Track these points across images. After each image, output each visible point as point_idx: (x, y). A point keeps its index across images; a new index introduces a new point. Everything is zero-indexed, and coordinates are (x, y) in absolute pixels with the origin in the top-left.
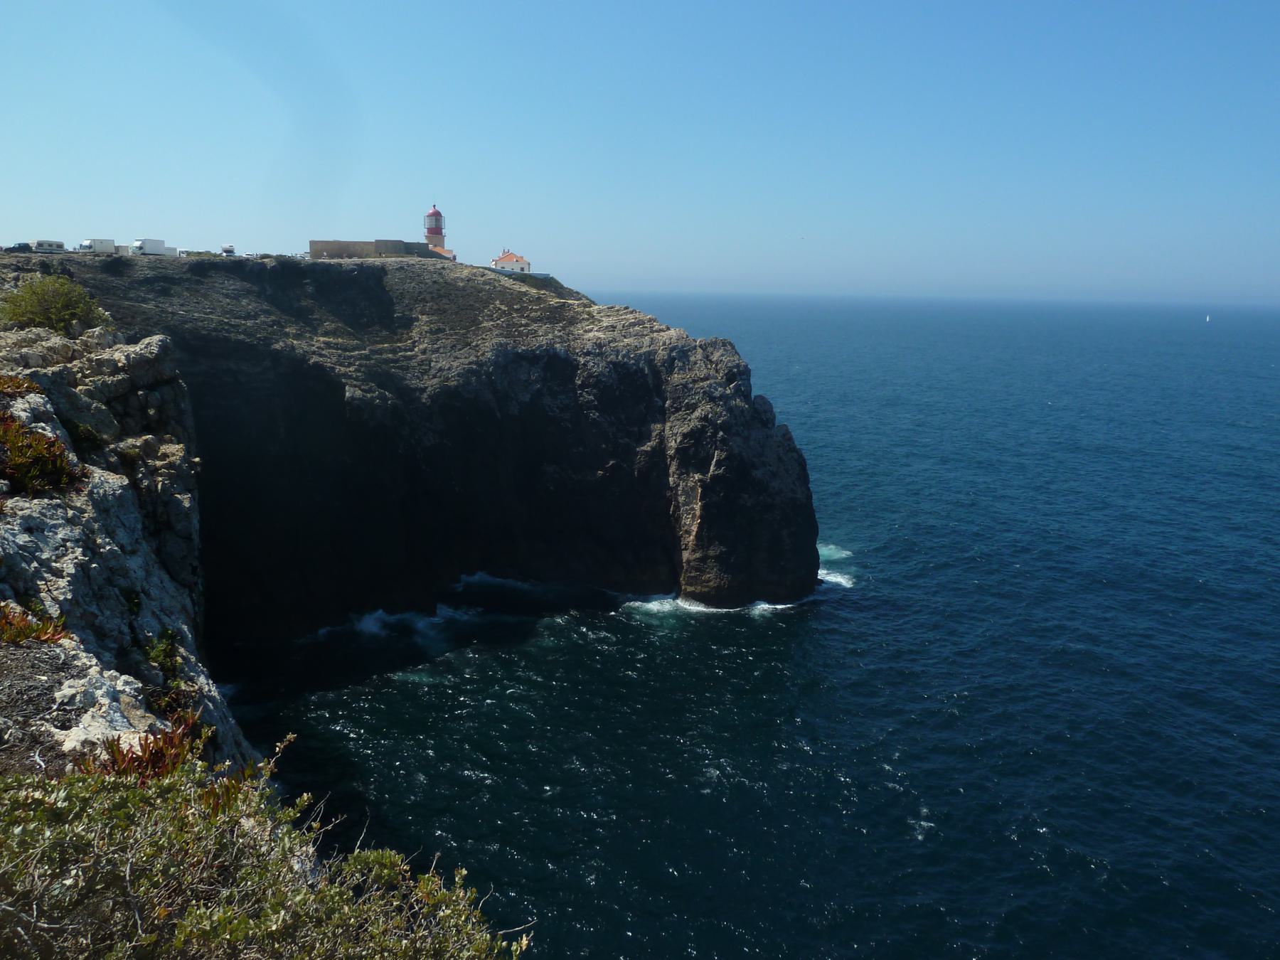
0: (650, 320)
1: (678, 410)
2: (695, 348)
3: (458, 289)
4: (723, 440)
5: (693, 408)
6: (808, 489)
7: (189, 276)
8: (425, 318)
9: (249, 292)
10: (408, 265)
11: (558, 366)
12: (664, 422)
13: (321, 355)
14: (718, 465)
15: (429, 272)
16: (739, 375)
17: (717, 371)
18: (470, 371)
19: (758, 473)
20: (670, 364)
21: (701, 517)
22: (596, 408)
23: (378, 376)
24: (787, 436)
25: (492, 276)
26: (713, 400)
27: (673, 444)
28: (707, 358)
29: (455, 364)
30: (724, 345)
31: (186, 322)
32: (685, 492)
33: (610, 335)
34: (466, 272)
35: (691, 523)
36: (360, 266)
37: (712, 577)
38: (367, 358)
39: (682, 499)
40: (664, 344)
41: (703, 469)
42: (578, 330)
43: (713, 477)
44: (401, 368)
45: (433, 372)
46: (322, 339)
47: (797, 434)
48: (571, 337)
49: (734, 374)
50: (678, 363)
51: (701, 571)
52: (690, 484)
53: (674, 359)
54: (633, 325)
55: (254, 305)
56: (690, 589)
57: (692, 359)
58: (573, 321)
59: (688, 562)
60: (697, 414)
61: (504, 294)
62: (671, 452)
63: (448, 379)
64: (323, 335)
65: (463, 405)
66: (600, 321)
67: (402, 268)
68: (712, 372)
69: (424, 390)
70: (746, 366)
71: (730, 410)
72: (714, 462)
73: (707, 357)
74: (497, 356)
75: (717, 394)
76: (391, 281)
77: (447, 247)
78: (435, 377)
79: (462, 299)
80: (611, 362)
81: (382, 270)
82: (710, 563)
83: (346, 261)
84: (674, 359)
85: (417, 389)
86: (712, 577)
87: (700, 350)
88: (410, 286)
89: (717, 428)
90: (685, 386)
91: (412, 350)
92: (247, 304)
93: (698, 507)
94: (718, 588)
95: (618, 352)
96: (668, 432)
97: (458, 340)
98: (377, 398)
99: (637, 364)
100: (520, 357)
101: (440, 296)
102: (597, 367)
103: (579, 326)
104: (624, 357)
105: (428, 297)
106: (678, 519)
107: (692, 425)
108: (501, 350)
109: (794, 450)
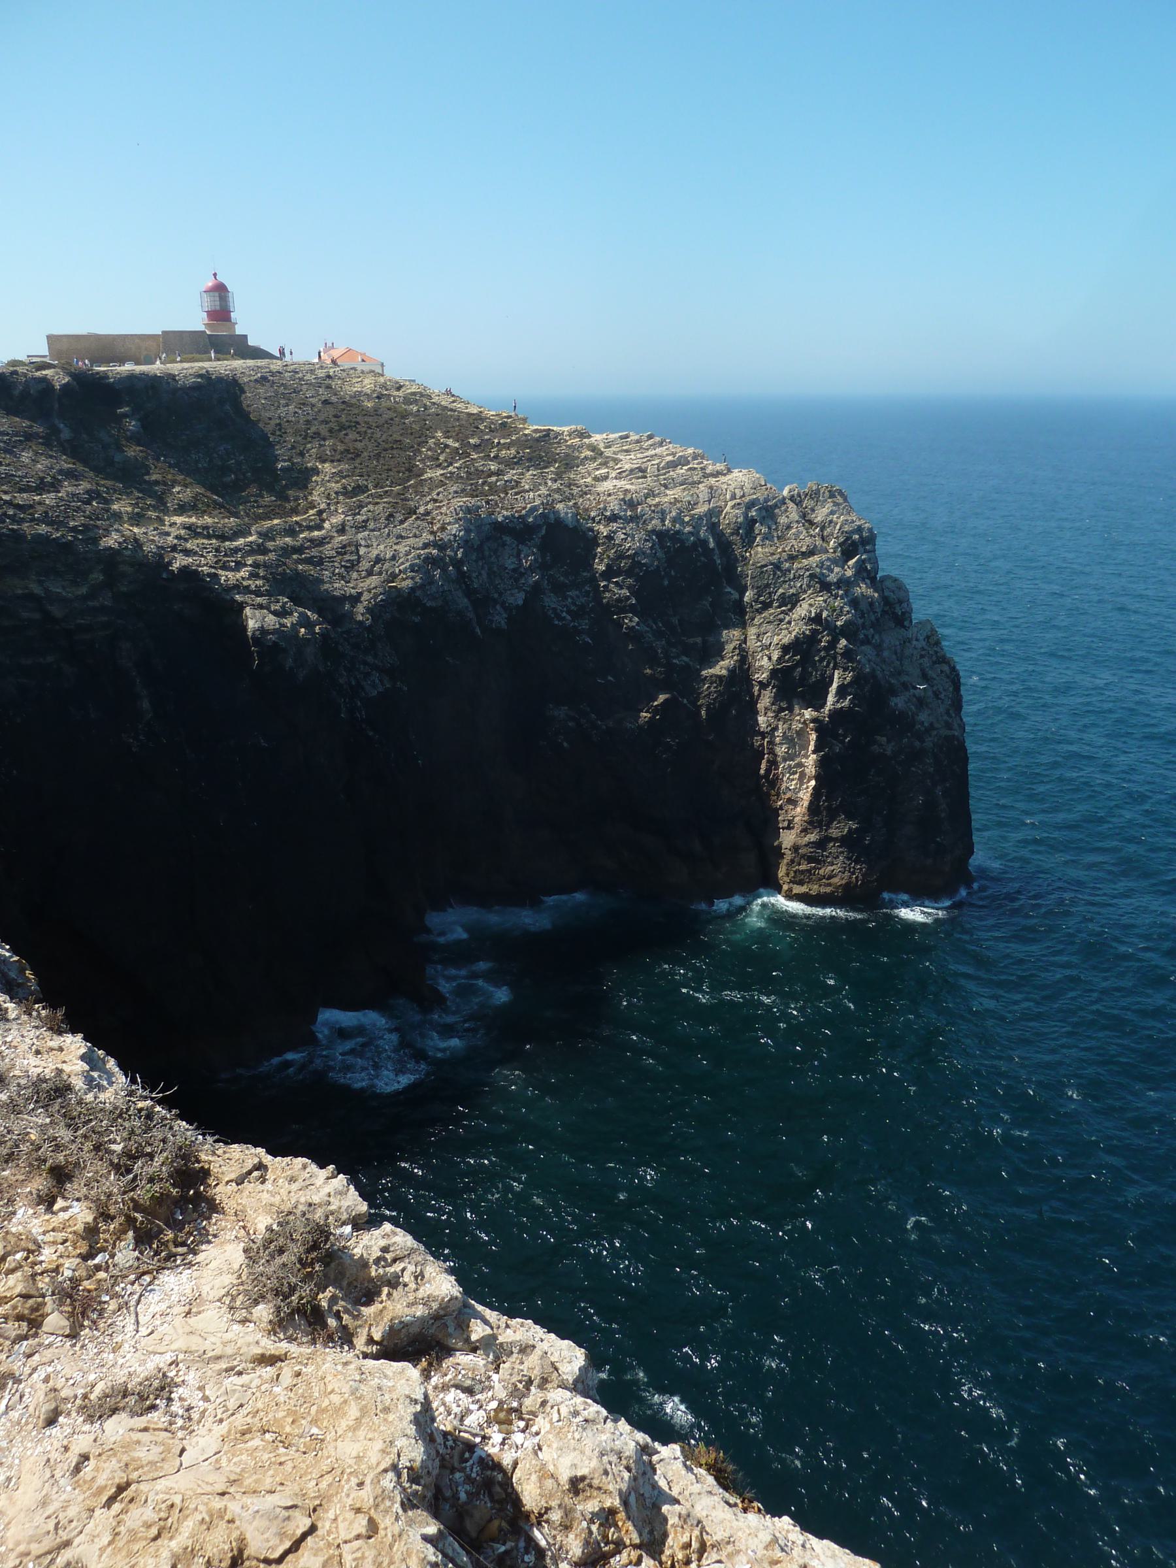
0: (695, 457)
1: (766, 606)
3: (366, 413)
4: (848, 654)
5: (792, 601)
9: (29, 437)
10: (273, 374)
11: (563, 542)
12: (743, 625)
13: (187, 552)
14: (842, 692)
17: (823, 539)
18: (428, 559)
19: (898, 702)
21: (817, 778)
22: (633, 609)
23: (290, 584)
24: (933, 640)
26: (825, 586)
27: (765, 662)
29: (402, 549)
30: (832, 496)
34: (368, 384)
37: (837, 870)
38: (261, 550)
39: (781, 750)
40: (733, 497)
41: (815, 698)
42: (584, 475)
43: (834, 714)
44: (309, 561)
45: (365, 565)
46: (179, 520)
49: (854, 543)
52: (797, 726)
53: (754, 521)
54: (673, 465)
55: (47, 462)
56: (798, 890)
57: (783, 520)
58: (569, 463)
59: (795, 848)
60: (802, 610)
62: (763, 676)
63: (393, 577)
66: (617, 461)
67: (264, 378)
68: (819, 542)
69: (356, 599)
71: (854, 603)
72: (835, 685)
73: (804, 516)
74: (468, 531)
75: (832, 578)
76: (255, 401)
78: (370, 573)
79: (385, 433)
80: (653, 531)
81: (231, 388)
83: (175, 368)
84: (754, 521)
85: (344, 598)
86: (837, 870)
87: (791, 505)
88: (287, 411)
90: (777, 566)
91: (319, 527)
92: (34, 462)
93: (810, 761)
94: (847, 887)
95: (663, 512)
96: (752, 643)
99: (695, 533)
100: (500, 529)
101: (342, 427)
102: (632, 540)
104: (674, 521)
106: (774, 782)
109: (943, 660)
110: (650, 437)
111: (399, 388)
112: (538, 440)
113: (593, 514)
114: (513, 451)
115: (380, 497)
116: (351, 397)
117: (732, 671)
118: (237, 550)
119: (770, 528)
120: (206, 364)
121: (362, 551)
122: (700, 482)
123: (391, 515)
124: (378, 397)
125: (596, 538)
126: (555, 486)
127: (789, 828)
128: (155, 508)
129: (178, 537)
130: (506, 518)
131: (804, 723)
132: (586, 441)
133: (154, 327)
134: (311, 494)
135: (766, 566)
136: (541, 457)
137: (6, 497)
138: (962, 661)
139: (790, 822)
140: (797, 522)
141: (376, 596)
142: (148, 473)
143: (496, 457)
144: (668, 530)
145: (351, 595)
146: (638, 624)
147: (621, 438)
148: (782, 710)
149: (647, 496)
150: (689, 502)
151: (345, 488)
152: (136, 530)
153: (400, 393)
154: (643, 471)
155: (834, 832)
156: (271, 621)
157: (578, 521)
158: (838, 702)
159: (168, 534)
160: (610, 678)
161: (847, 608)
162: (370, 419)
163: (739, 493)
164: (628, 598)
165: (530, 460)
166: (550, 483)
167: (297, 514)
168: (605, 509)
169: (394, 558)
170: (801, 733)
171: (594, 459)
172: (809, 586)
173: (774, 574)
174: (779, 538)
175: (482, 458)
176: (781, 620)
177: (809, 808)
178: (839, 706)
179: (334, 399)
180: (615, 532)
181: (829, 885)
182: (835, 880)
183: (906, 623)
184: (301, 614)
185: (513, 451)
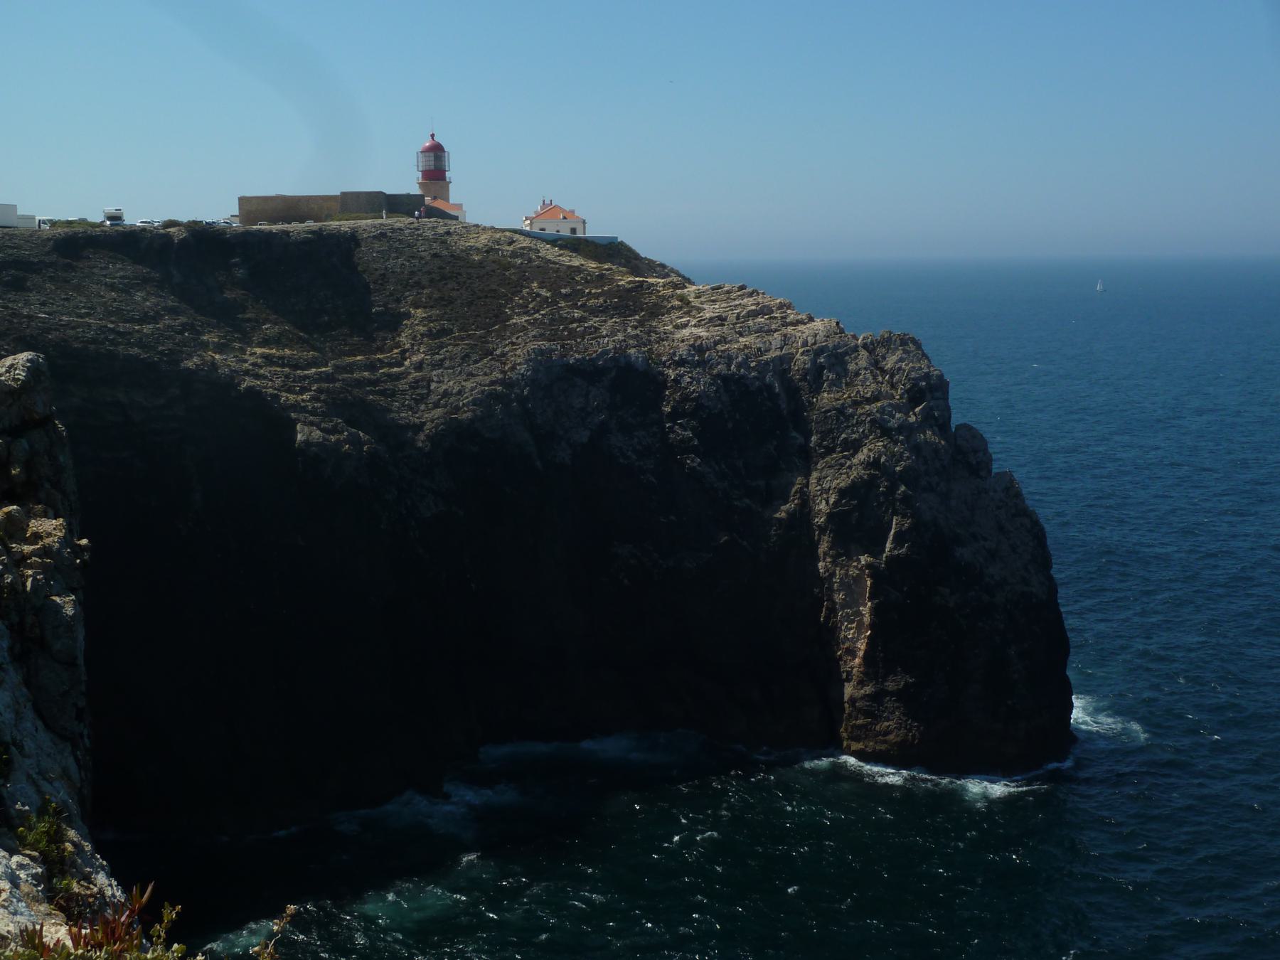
0: (781, 306)
1: (830, 451)
2: (856, 349)
4: (905, 499)
5: (854, 446)
6: (1051, 578)
7: (54, 257)
8: (420, 313)
9: (146, 280)
10: (393, 230)
11: (634, 383)
13: (257, 377)
15: (426, 239)
16: (929, 392)
17: (893, 386)
18: (493, 396)
20: (815, 377)
21: (872, 626)
23: (347, 406)
24: (1011, 490)
25: (525, 242)
26: (886, 432)
27: (823, 506)
28: (876, 365)
29: (469, 385)
31: (48, 331)
32: (845, 586)
33: (716, 332)
34: (484, 239)
35: (856, 639)
36: (318, 234)
37: (892, 725)
38: (329, 378)
39: (839, 597)
40: (805, 344)
41: (875, 548)
42: (665, 325)
43: (891, 559)
44: (383, 393)
45: (433, 398)
46: (259, 351)
47: (1031, 487)
48: (654, 337)
50: (829, 375)
51: (876, 718)
54: (754, 314)
55: (154, 300)
57: (852, 367)
58: (657, 311)
59: (853, 700)
60: (862, 456)
61: (547, 273)
62: (820, 520)
63: (457, 409)
64: (260, 345)
65: (479, 453)
66: (700, 310)
67: (383, 235)
68: (885, 388)
69: (419, 428)
70: (941, 377)
71: (916, 449)
74: (535, 371)
75: (893, 423)
77: (454, 197)
78: (436, 405)
79: (479, 280)
80: (719, 375)
82: (889, 703)
83: (294, 227)
84: (822, 367)
87: (863, 353)
89: (895, 480)
90: (841, 411)
91: (400, 364)
92: (143, 299)
93: (866, 610)
95: (730, 359)
96: (814, 487)
97: (473, 347)
98: (346, 441)
101: (444, 278)
102: (696, 384)
103: (666, 318)
104: (739, 366)
105: (425, 281)
106: (835, 630)
107: (854, 474)
108: (541, 361)
110: (742, 288)
111: (511, 242)
112: (629, 290)
113: (664, 359)
114: (601, 300)
115: (462, 339)
116: (462, 251)
117: (791, 515)
118: (306, 377)
119: (837, 374)
120: (380, 221)
121: (433, 386)
122: (776, 330)
123: (467, 356)
124: (487, 252)
125: (665, 381)
126: (634, 332)
127: (848, 680)
128: (240, 340)
129: (254, 364)
130: (577, 360)
131: (861, 569)
132: (679, 292)
133: (335, 191)
134: (399, 335)
135: (829, 411)
136: (627, 306)
137: (111, 326)
138: (1044, 514)
139: (849, 673)
140: (866, 369)
141: (436, 427)
142: (244, 312)
143: (583, 305)
144: (734, 374)
145: (415, 424)
146: (699, 465)
147: (713, 289)
148: (839, 555)
149: (716, 343)
150: (759, 349)
151: (430, 330)
152: (217, 357)
153: (511, 248)
154: (725, 319)
155: (890, 686)
156: (317, 434)
157: (649, 365)
158: (895, 548)
159: (246, 361)
160: (673, 518)
161: (907, 454)
162: (470, 270)
163: (810, 340)
164: (690, 439)
165: (615, 308)
166: (629, 330)
167: (382, 353)
168: (674, 354)
169: (460, 393)
170: (858, 580)
171: (680, 308)
172: (871, 432)
173: (838, 419)
174: (847, 384)
175: (568, 307)
176: (842, 465)
177: (865, 658)
178: (896, 552)
179: (445, 253)
180: (682, 376)
181: (885, 742)
182: (891, 737)
183: (983, 473)
184: (350, 434)
185: (601, 300)
